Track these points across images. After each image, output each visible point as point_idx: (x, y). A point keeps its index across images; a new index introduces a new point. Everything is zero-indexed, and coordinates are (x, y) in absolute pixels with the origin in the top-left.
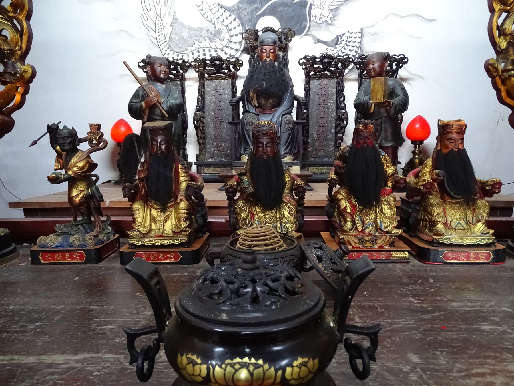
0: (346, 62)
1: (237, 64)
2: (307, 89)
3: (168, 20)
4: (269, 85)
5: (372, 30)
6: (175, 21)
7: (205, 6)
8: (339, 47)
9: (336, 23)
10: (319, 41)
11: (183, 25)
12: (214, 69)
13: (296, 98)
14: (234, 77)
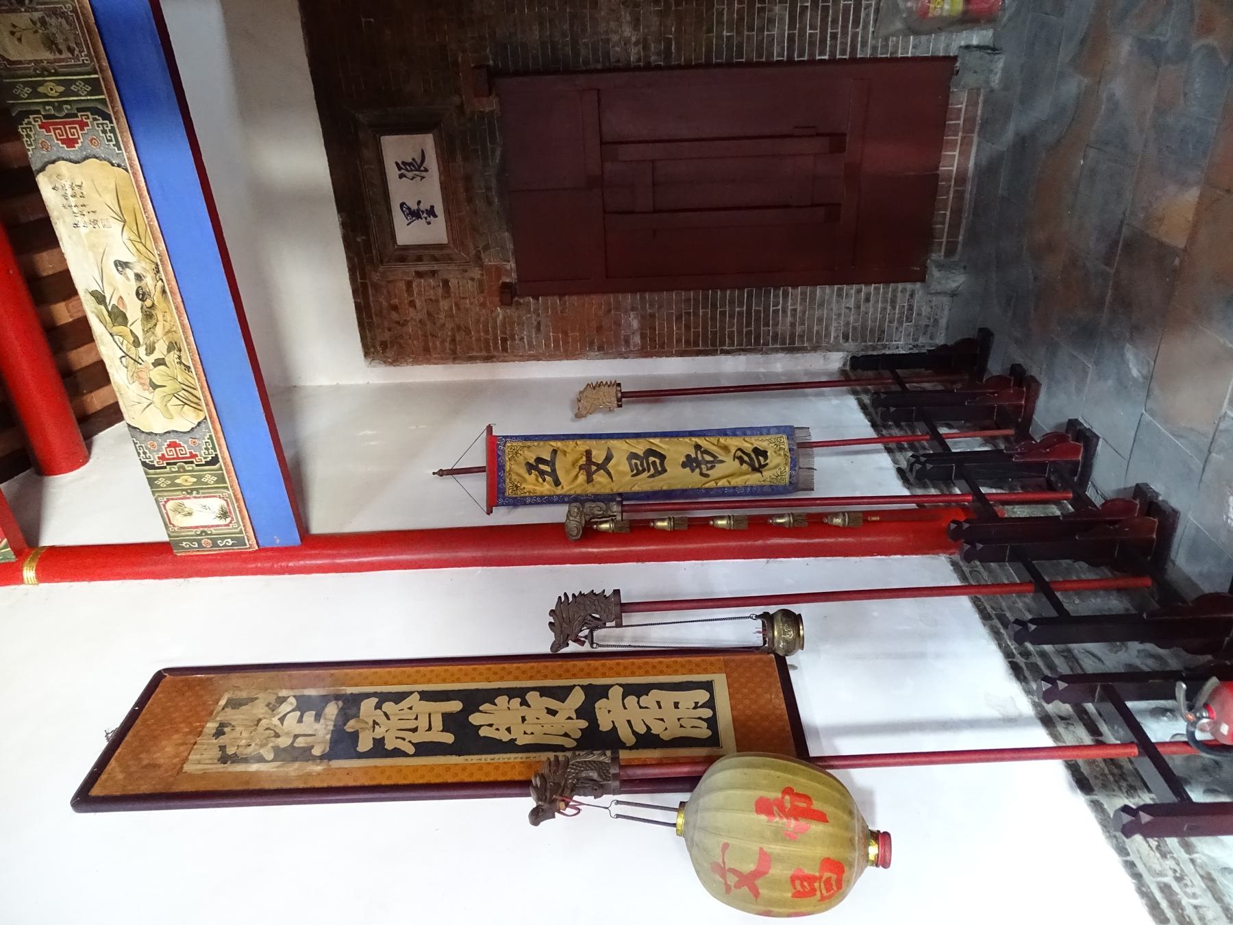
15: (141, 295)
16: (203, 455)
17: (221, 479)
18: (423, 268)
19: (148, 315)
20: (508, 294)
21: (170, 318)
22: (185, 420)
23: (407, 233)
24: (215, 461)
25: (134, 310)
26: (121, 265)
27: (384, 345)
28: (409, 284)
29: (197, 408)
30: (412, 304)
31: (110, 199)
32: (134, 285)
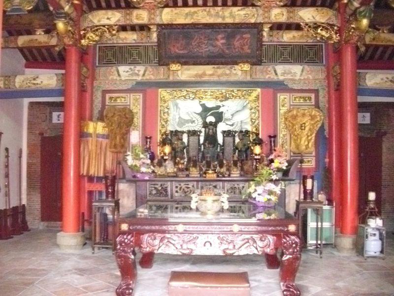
0: (236, 132)
1: (200, 132)
2: (224, 140)
3: (177, 117)
4: (211, 139)
5: (245, 121)
6: (180, 118)
7: (190, 113)
8: (234, 126)
9: (233, 119)
10: (227, 124)
11: (182, 118)
12: (193, 133)
13: (219, 144)
14: (199, 136)
15: (37, 84)
16: (11, 86)
17: (6, 88)
18: (48, 117)
19: (34, 84)
20: (41, 134)
21: (33, 87)
22: (17, 85)
23: (55, 115)
24: (10, 88)
25: (35, 82)
26: (42, 82)
27: (32, 106)
28: (44, 114)
29: (19, 88)
30: (41, 114)
31: (51, 83)
32: (39, 83)
